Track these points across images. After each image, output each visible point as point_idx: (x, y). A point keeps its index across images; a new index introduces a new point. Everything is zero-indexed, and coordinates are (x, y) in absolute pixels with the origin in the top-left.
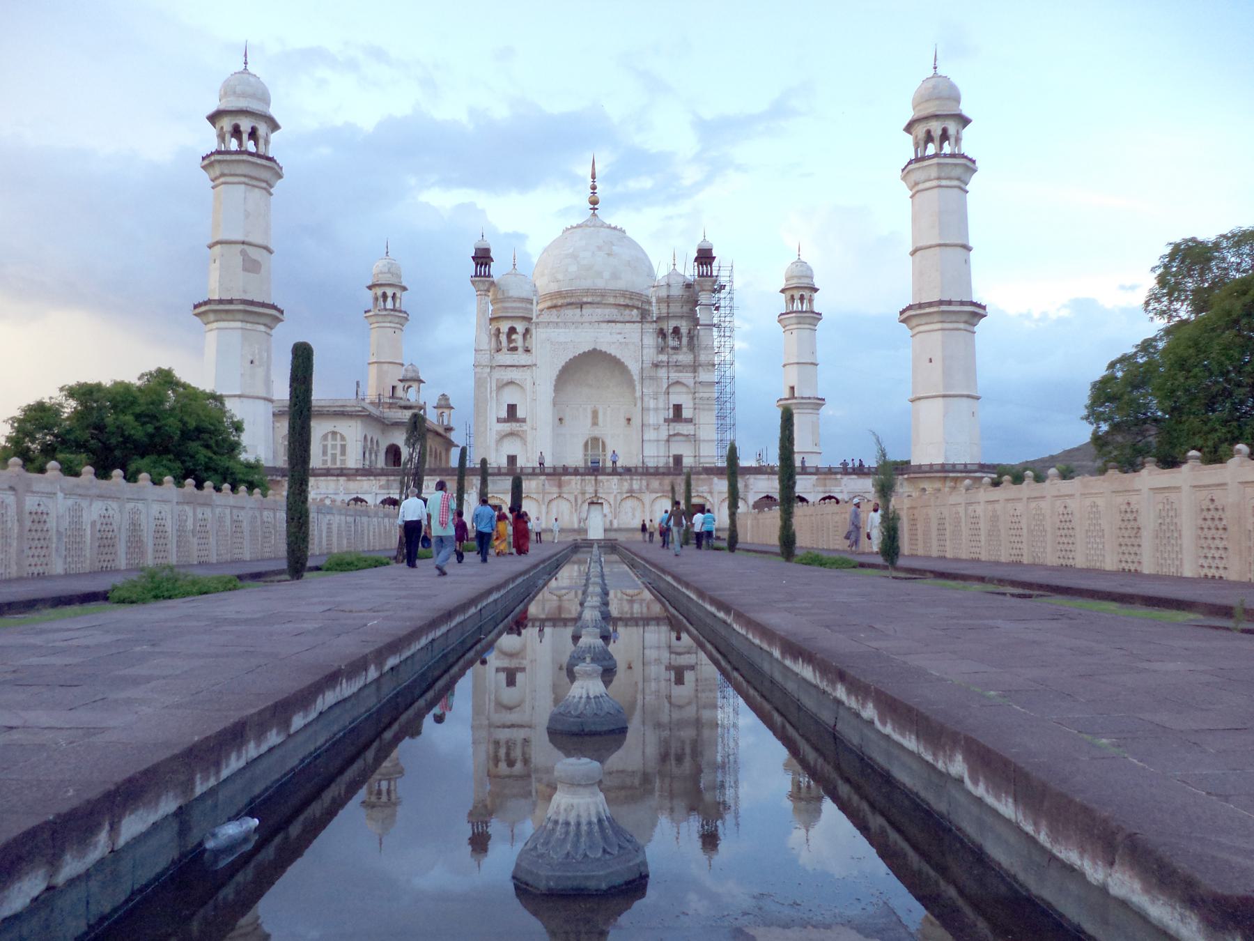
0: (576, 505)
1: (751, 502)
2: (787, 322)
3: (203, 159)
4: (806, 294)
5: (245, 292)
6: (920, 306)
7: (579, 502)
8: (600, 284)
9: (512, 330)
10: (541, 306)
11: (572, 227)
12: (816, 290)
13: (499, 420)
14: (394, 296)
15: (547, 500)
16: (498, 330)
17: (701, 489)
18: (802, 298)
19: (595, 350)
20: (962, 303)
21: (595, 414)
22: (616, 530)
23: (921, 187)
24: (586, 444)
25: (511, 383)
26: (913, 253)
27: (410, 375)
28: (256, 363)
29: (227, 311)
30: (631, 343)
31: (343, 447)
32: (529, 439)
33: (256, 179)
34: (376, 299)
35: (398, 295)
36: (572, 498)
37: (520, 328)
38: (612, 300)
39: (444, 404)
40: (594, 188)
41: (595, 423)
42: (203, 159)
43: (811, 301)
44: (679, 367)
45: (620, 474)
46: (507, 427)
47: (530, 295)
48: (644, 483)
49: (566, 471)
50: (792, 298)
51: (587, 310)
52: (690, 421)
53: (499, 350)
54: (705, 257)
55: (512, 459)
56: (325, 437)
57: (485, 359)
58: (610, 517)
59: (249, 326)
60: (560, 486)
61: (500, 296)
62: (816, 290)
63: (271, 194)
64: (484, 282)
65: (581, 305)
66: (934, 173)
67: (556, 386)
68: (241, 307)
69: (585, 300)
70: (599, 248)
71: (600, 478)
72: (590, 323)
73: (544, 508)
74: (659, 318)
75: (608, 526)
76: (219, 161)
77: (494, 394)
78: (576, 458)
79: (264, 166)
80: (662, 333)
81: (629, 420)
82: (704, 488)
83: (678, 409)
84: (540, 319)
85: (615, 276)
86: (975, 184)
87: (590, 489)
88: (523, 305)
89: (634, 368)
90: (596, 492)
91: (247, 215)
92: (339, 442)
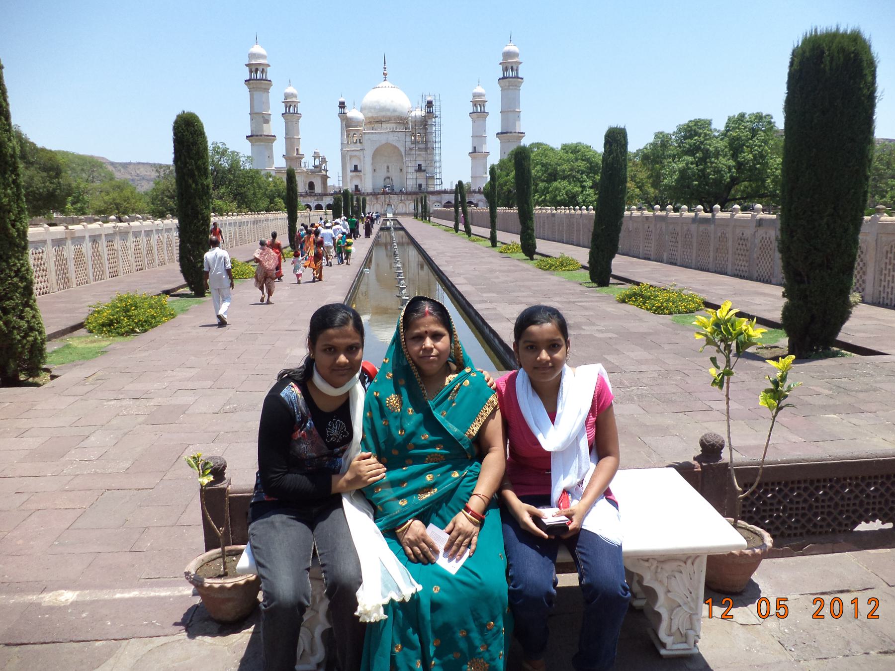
0: (382, 206)
6: (502, 133)
8: (389, 114)
19: (387, 144)
21: (388, 167)
25: (355, 156)
30: (401, 141)
39: (324, 160)
41: (388, 171)
49: (379, 194)
51: (384, 125)
55: (356, 186)
67: (373, 158)
83: (420, 165)
89: (402, 150)
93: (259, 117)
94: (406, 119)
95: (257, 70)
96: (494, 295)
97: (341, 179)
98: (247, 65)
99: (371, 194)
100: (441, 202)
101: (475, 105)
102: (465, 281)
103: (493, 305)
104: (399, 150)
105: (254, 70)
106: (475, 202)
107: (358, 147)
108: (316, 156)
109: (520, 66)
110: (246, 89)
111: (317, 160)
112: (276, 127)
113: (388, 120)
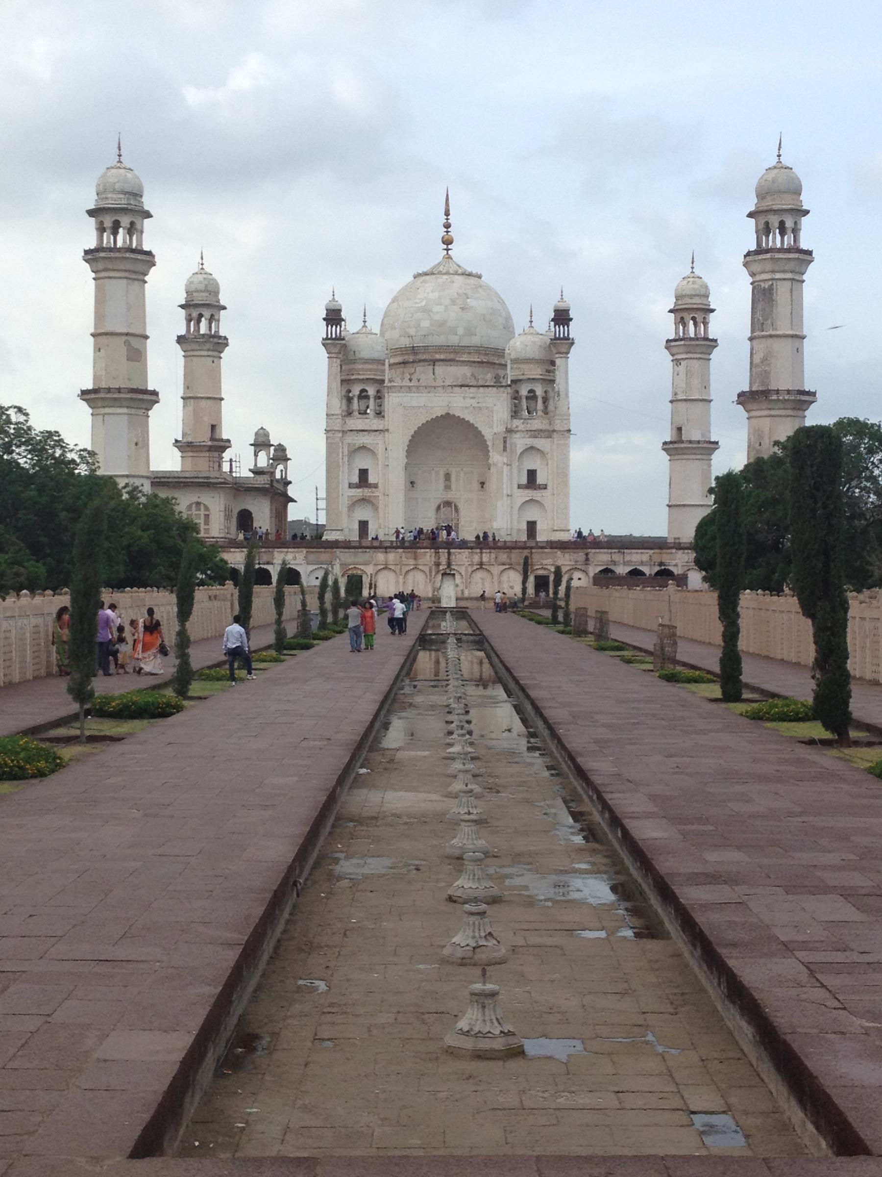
0: (430, 578)
1: (591, 574)
2: (674, 350)
3: (87, 252)
4: (699, 317)
5: (129, 379)
7: (433, 573)
8: (454, 340)
9: (363, 395)
10: (392, 361)
11: (426, 274)
12: (713, 311)
13: (351, 486)
14: (211, 319)
15: (403, 573)
16: (349, 391)
17: (545, 562)
18: (694, 319)
19: (448, 414)
20: (789, 392)
21: (448, 477)
22: (467, 599)
23: (758, 278)
24: (439, 508)
25: (363, 448)
26: (751, 339)
27: (261, 439)
28: (140, 444)
29: (115, 399)
31: (207, 516)
32: (381, 505)
33: (135, 272)
34: (189, 320)
35: (216, 317)
36: (427, 569)
37: (371, 391)
38: (465, 358)
39: (281, 456)
40: (447, 226)
41: (448, 487)
42: (87, 252)
43: (706, 324)
44: (536, 433)
45: (472, 548)
46: (358, 493)
47: (383, 357)
48: (493, 556)
50: (682, 318)
51: (440, 369)
52: (545, 487)
53: (349, 414)
54: (562, 317)
55: (363, 526)
56: (189, 507)
57: (337, 424)
58: (461, 587)
59: (133, 411)
60: (415, 559)
61: (351, 357)
62: (713, 311)
63: (146, 282)
64: (335, 345)
65: (434, 362)
66: (769, 266)
68: (129, 396)
69: (438, 356)
70: (453, 302)
71: (452, 550)
72: (443, 387)
73: (401, 577)
74: (512, 381)
75: (460, 595)
76: (104, 258)
77: (346, 459)
78: (428, 523)
79: (142, 260)
80: (516, 397)
81: (483, 484)
82: (550, 561)
83: (532, 474)
84: (393, 384)
85: (469, 332)
86: (811, 274)
87: (443, 560)
88: (375, 367)
89: (487, 434)
90: (449, 565)
91: (129, 308)
92: (202, 512)
93: (120, 340)
94: (500, 352)
95: (116, 226)
96: (735, 856)
97: (322, 504)
98: (91, 213)
99: (401, 544)
100: (585, 572)
101: (682, 321)
102: (651, 808)
103: (741, 889)
104: (477, 434)
105: (108, 222)
106: (676, 571)
107: (376, 424)
108: (261, 443)
109: (805, 222)
110: (86, 272)
111: (262, 455)
112: (165, 368)
113: (450, 355)
